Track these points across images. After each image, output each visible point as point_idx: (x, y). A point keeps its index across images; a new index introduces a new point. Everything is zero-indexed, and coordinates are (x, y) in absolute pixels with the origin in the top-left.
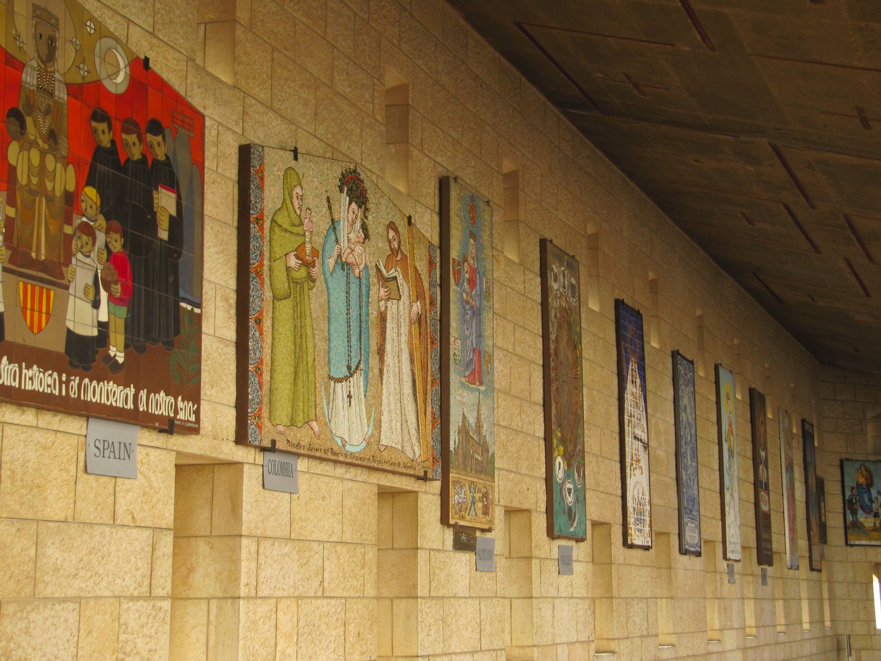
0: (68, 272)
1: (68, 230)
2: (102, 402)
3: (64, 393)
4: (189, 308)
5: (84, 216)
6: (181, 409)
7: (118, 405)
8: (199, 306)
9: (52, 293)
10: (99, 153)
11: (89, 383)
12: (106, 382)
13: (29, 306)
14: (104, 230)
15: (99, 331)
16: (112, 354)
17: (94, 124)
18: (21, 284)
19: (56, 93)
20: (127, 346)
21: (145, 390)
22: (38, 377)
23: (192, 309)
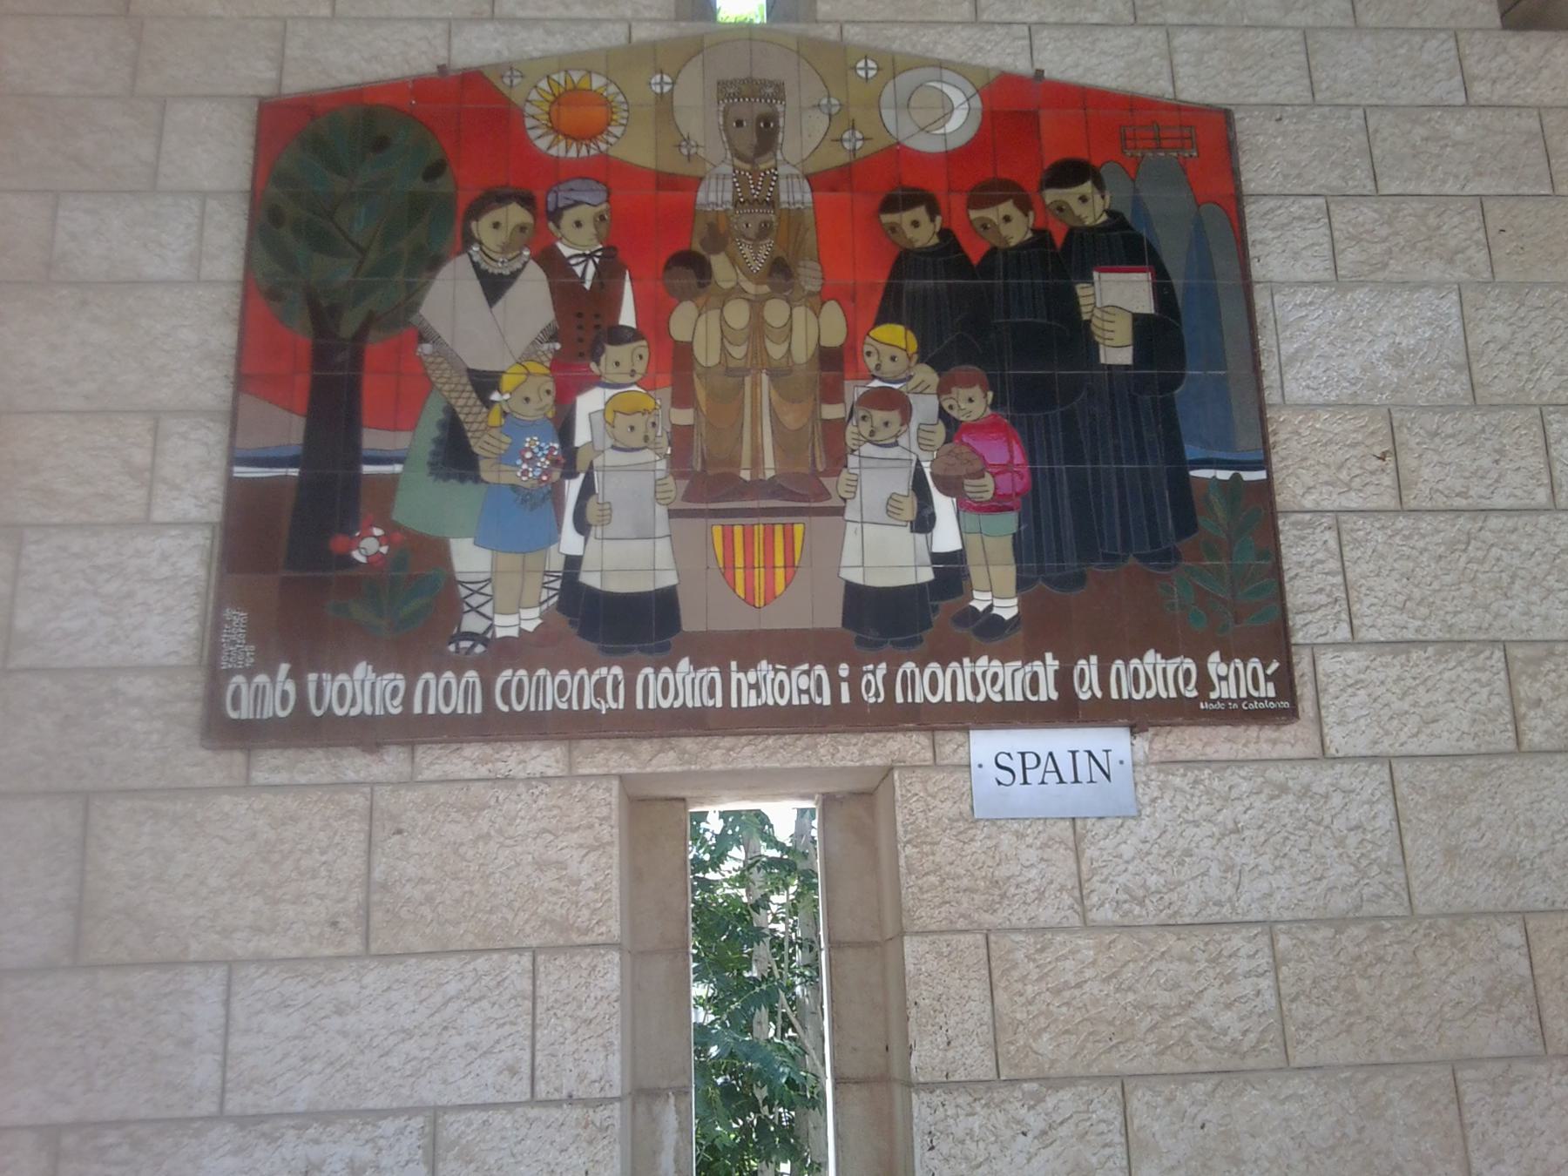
0: (838, 486)
1: (832, 412)
2: (960, 698)
3: (845, 699)
4: (1224, 475)
5: (874, 377)
6: (1221, 678)
7: (1009, 697)
8: (1263, 463)
9: (798, 529)
10: (907, 262)
11: (917, 671)
12: (966, 661)
13: (739, 562)
14: (933, 389)
15: (935, 570)
16: (981, 607)
17: (887, 218)
18: (717, 532)
19: (783, 197)
20: (1022, 584)
21: (1094, 659)
22: (773, 680)
23: (1236, 478)
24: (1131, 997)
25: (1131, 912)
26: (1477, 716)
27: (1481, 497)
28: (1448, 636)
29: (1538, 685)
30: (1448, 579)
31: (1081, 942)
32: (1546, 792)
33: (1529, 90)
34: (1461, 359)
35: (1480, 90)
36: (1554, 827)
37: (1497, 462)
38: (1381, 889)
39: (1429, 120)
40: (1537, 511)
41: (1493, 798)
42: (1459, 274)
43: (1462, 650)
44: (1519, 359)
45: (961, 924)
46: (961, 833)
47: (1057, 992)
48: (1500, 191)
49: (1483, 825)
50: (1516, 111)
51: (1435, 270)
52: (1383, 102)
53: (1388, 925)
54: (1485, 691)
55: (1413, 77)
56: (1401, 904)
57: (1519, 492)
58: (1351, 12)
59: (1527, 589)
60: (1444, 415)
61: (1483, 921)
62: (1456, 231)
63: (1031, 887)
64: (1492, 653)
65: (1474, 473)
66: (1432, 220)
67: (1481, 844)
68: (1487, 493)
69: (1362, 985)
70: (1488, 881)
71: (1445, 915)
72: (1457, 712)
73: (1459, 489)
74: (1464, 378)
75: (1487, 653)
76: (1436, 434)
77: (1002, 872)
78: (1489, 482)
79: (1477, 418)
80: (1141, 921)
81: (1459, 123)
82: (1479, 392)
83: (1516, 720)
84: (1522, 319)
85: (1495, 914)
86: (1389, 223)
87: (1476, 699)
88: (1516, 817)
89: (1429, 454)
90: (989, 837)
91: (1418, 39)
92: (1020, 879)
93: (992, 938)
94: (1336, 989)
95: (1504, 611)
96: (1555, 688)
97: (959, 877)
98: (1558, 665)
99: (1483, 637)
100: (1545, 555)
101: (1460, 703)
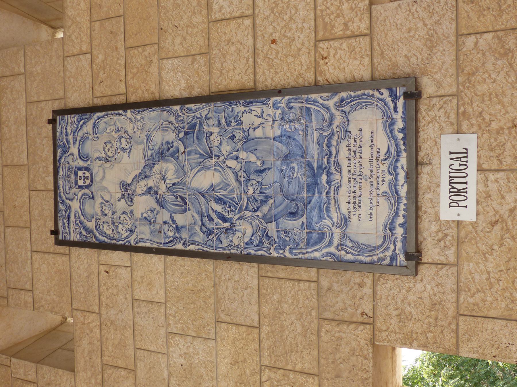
24: (496, 247)
25: (450, 241)
26: (352, 56)
27: (248, 51)
28: (313, 69)
29: (337, 25)
30: (286, 68)
31: (466, 268)
32: (392, 21)
33: (85, 26)
34: (190, 59)
35: (85, 47)
36: (411, 17)
37: (233, 43)
38: (442, 111)
39: (97, 69)
40: (254, 24)
41: (395, 49)
42: (155, 59)
43: (319, 63)
44: (189, 32)
45: (453, 327)
46: (407, 317)
47: (491, 286)
48: (123, 40)
49: (409, 55)
50: (92, 32)
51: (154, 70)
52: (91, 89)
53: (462, 109)
54: (340, 52)
55: (82, 76)
56: (451, 101)
57: (246, 33)
58: (60, 100)
59: (290, 30)
60: (213, 68)
61: (462, 57)
62: (139, 60)
63: (436, 289)
64: (321, 48)
65: (238, 54)
66: (135, 70)
67: (419, 56)
68: (246, 48)
69: (494, 125)
70: (439, 53)
71: (457, 78)
72: (350, 67)
73: (245, 61)
74: (198, 57)
75: (321, 50)
76: (221, 72)
77: (427, 302)
78: (242, 47)
79: (214, 52)
80: (456, 236)
81: (98, 57)
82: (203, 51)
83: (354, 36)
84: (173, 31)
85: (458, 50)
86: (137, 89)
87: (343, 57)
88: (405, 37)
89: (230, 75)
90: (409, 304)
91: (67, 73)
92: (431, 292)
93: (461, 312)
94: (496, 139)
95: (301, 41)
96: (338, 16)
97: (429, 323)
98: (327, 14)
99: (313, 51)
100: (274, 22)
101: (345, 65)
